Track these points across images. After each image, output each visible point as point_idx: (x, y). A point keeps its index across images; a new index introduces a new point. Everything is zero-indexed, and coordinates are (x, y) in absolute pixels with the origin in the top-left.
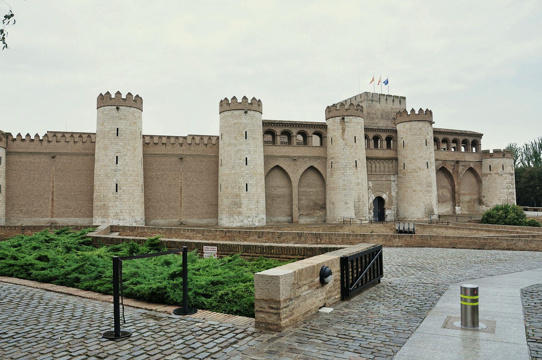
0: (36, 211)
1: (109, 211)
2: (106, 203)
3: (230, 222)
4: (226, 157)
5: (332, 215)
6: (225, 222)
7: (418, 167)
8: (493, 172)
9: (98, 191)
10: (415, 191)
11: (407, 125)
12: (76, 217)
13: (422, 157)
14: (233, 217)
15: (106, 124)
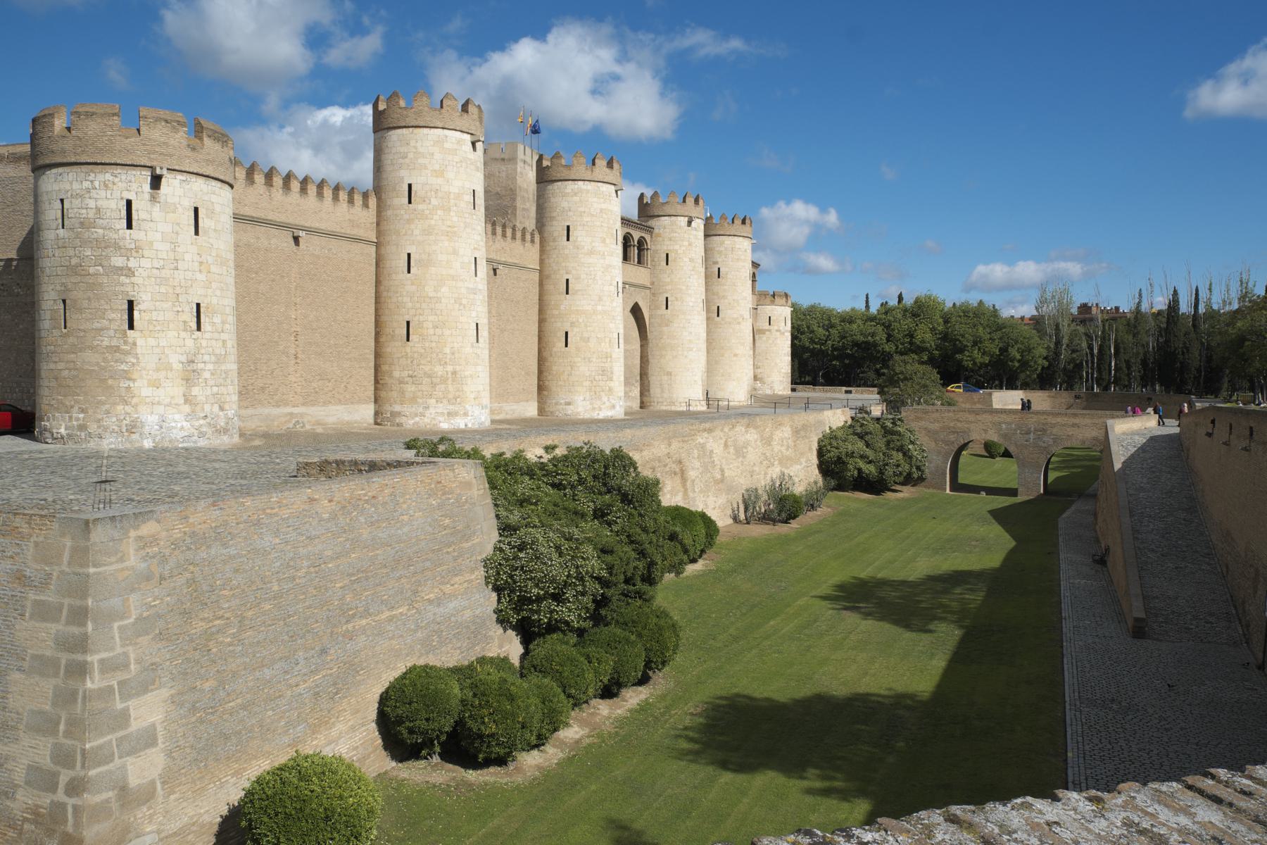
0: (263, 389)
1: (465, 388)
2: (458, 368)
3: (594, 409)
4: (583, 276)
5: (665, 395)
6: (580, 409)
7: (742, 316)
8: (774, 327)
9: (435, 338)
10: (736, 355)
11: (728, 241)
12: (340, 402)
13: (745, 298)
14: (600, 398)
15: (450, 175)
